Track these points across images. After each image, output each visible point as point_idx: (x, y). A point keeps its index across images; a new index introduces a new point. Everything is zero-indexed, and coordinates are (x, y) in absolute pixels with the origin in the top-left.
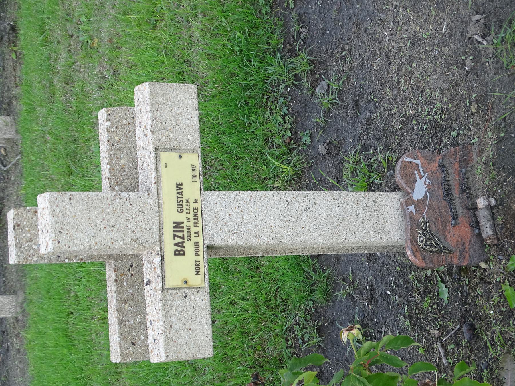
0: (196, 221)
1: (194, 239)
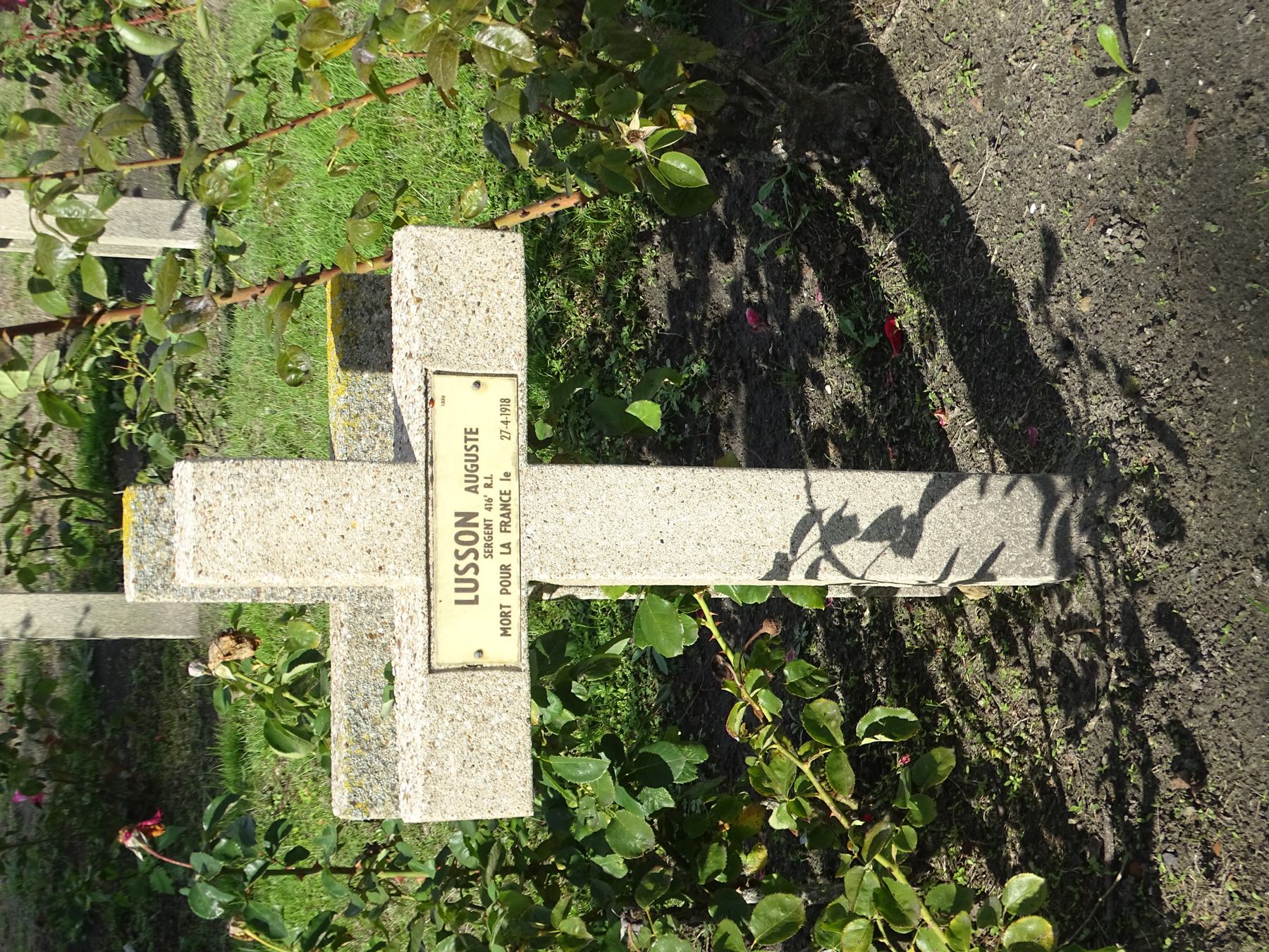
1: (499, 560)
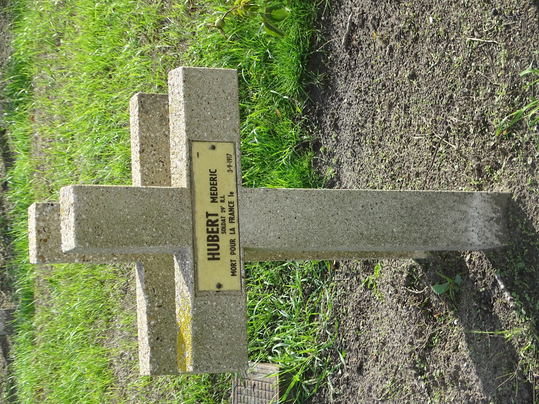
0: (232, 216)
